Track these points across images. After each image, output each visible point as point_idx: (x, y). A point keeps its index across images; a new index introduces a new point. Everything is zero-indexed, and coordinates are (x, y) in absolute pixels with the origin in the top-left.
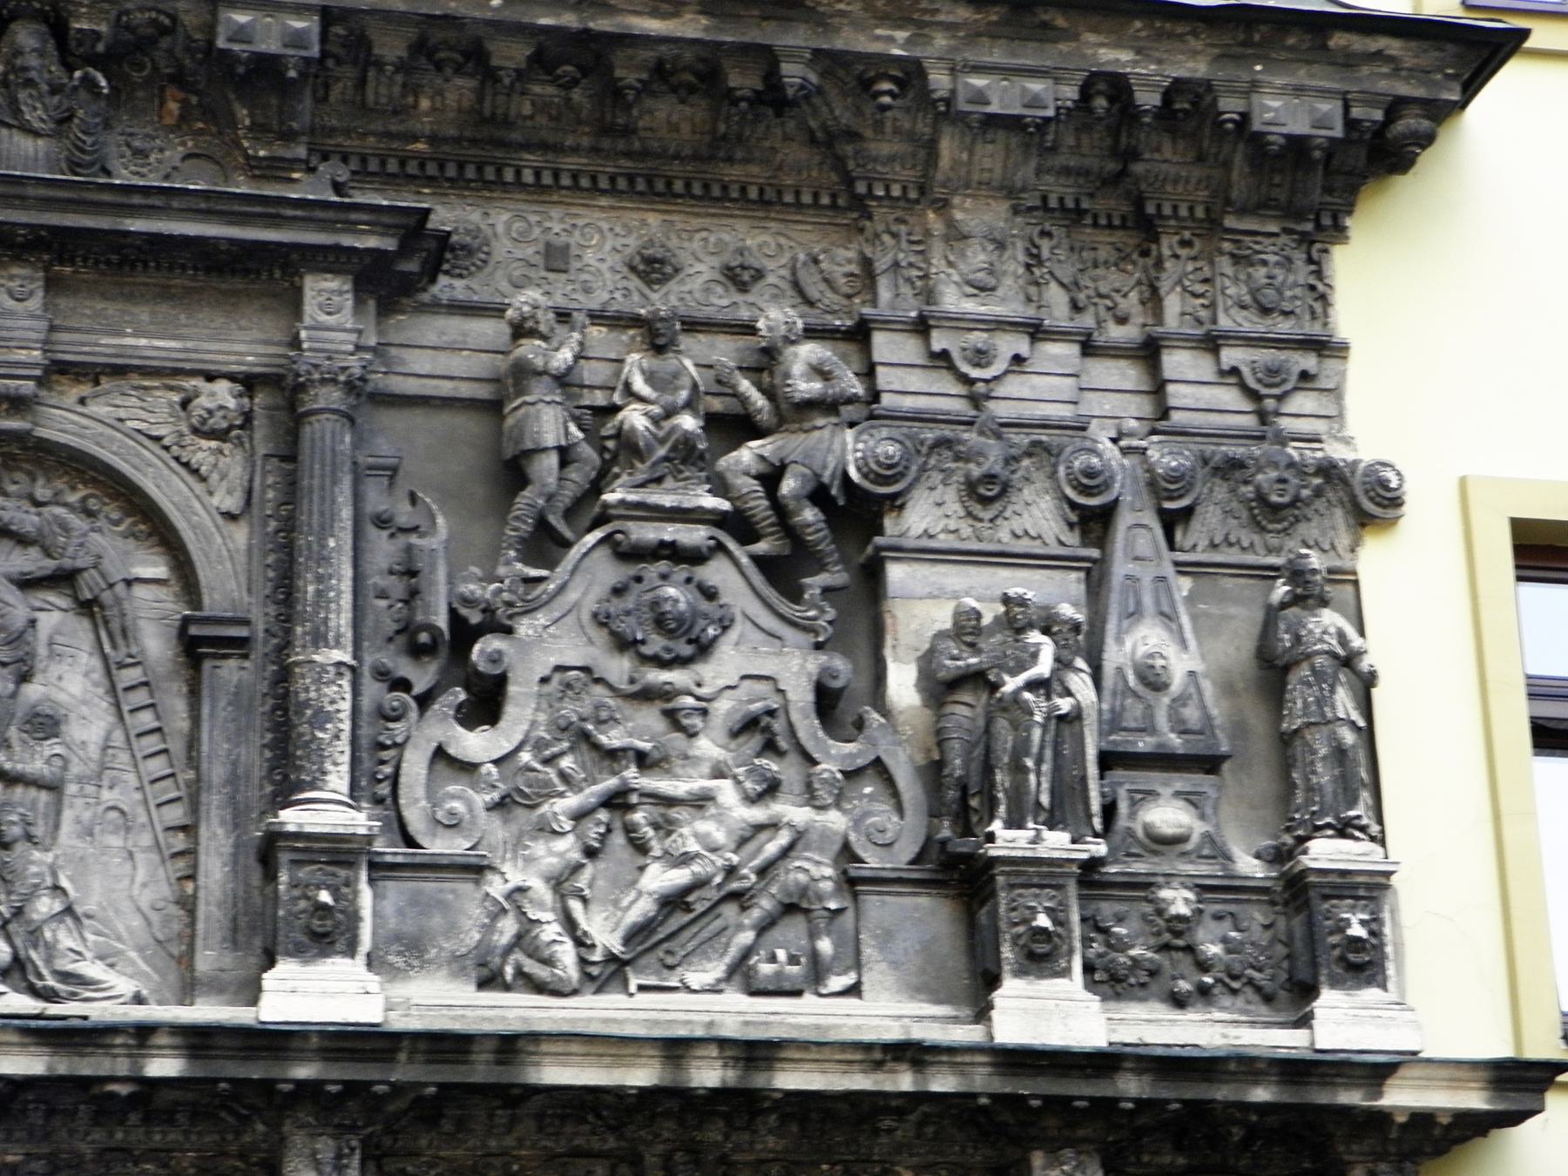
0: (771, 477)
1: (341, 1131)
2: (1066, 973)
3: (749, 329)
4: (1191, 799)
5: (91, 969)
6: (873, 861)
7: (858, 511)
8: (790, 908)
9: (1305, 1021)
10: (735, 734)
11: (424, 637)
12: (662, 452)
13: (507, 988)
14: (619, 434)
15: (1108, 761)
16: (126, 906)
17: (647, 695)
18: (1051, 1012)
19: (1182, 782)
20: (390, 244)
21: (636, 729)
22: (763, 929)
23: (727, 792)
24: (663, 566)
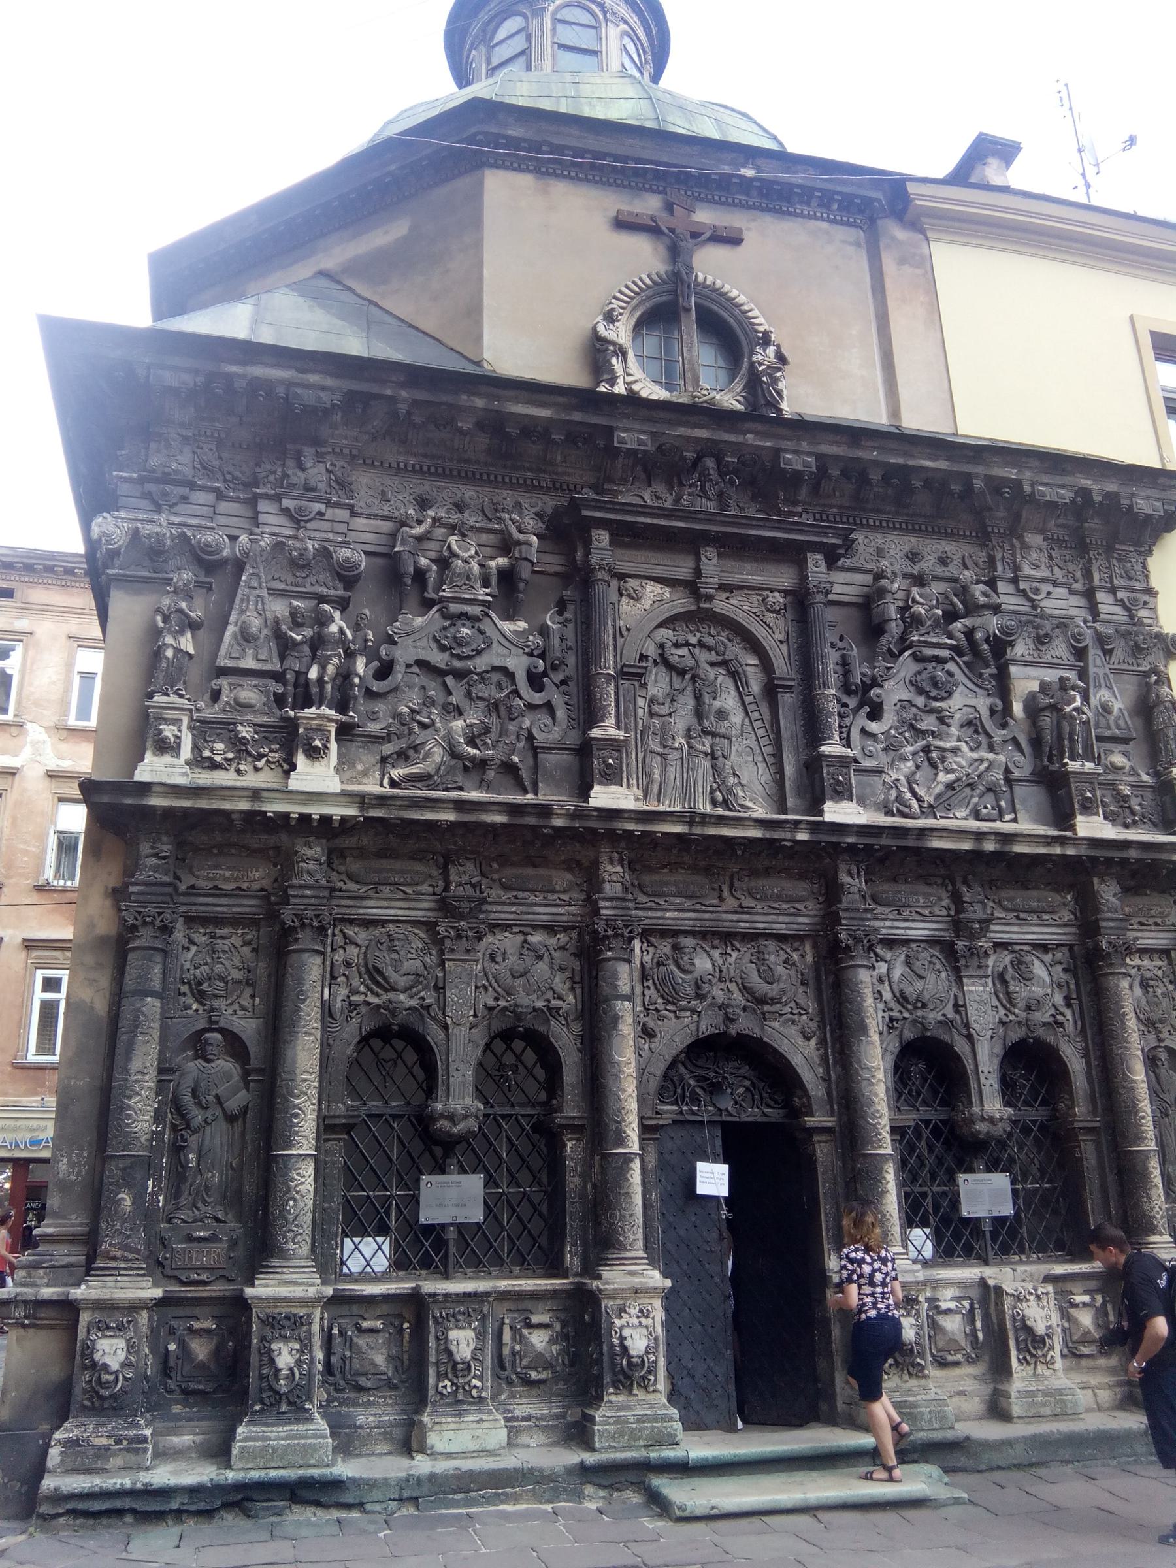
0: (969, 633)
1: (858, 863)
2: (1097, 814)
3: (956, 580)
4: (1126, 754)
5: (750, 804)
7: (1000, 645)
8: (989, 790)
10: (962, 726)
11: (854, 688)
12: (929, 623)
13: (893, 815)
14: (912, 616)
16: (757, 782)
17: (932, 711)
18: (1092, 826)
20: (839, 542)
21: (928, 723)
22: (981, 797)
24: (934, 664)
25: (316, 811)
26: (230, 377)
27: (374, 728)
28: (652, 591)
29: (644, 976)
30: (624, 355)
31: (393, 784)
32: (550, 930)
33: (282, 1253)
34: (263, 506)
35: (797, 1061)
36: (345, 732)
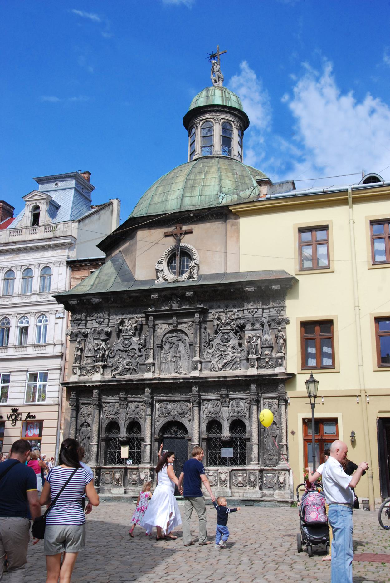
4: (269, 350)
5: (183, 371)
6: (242, 358)
15: (262, 348)
17: (224, 345)
18: (253, 372)
19: (268, 349)
23: (230, 353)
25: (94, 384)
26: (83, 300)
27: (110, 364)
29: (158, 410)
30: (162, 270)
32: (140, 402)
33: (90, 460)
34: (94, 321)
35: (186, 426)
36: (104, 367)
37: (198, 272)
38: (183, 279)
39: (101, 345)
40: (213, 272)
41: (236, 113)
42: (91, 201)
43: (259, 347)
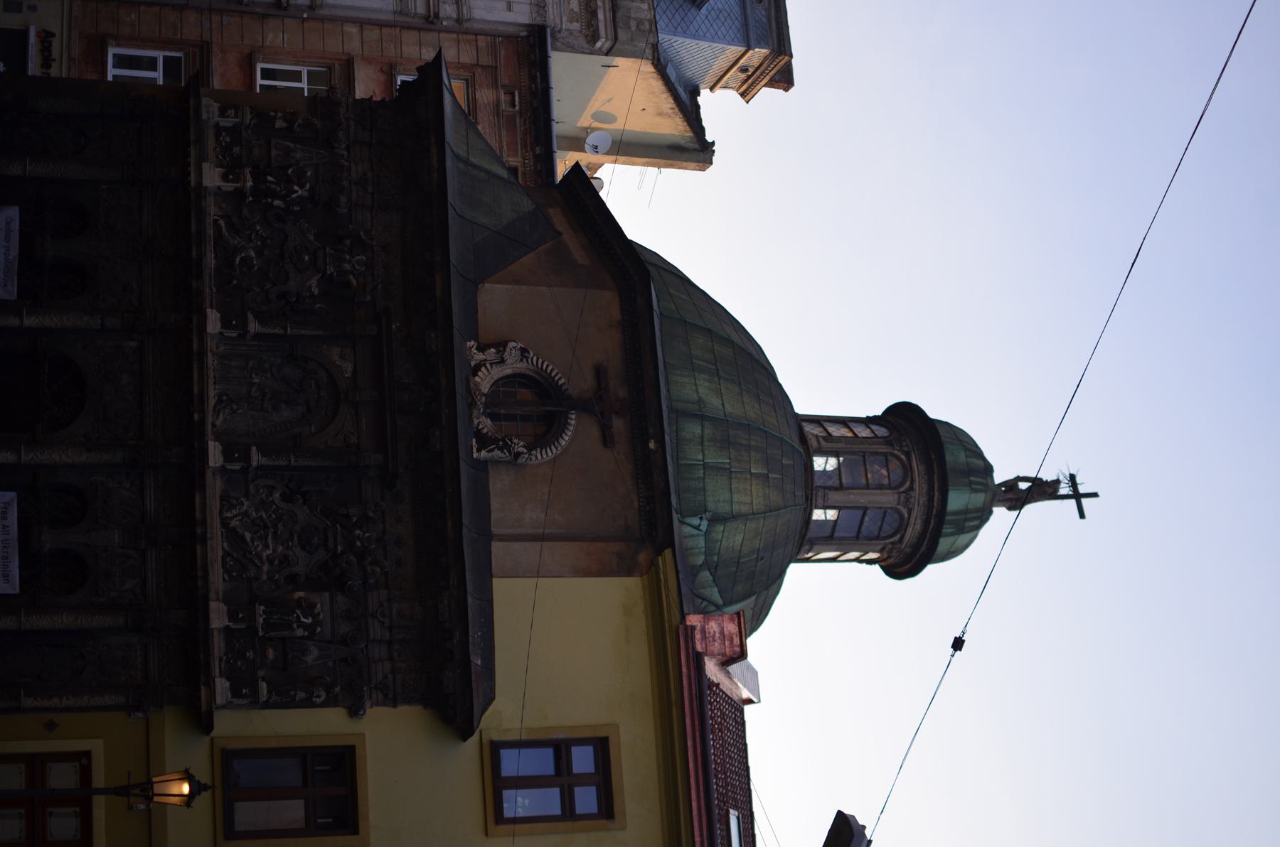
9: (221, 676)
18: (218, 617)
23: (269, 552)
25: (192, 169)
27: (245, 212)
28: (348, 367)
31: (216, 221)
37: (497, 462)
38: (476, 422)
39: (302, 186)
40: (495, 504)
41: (923, 549)
42: (712, 89)
43: (285, 633)
